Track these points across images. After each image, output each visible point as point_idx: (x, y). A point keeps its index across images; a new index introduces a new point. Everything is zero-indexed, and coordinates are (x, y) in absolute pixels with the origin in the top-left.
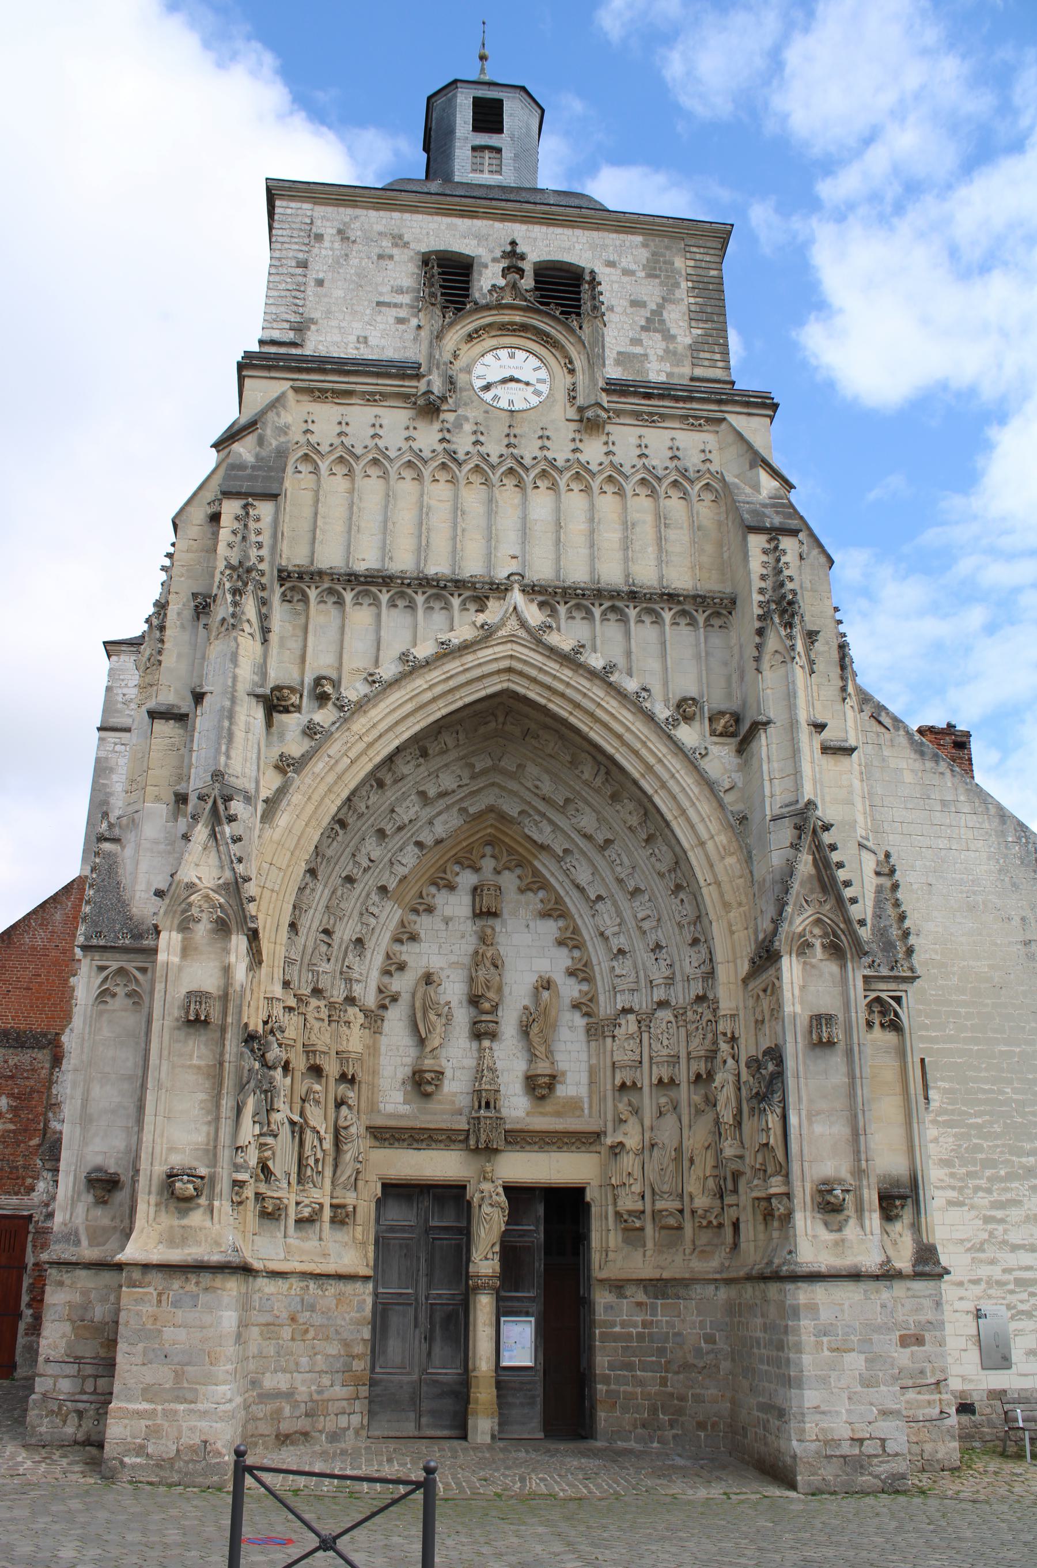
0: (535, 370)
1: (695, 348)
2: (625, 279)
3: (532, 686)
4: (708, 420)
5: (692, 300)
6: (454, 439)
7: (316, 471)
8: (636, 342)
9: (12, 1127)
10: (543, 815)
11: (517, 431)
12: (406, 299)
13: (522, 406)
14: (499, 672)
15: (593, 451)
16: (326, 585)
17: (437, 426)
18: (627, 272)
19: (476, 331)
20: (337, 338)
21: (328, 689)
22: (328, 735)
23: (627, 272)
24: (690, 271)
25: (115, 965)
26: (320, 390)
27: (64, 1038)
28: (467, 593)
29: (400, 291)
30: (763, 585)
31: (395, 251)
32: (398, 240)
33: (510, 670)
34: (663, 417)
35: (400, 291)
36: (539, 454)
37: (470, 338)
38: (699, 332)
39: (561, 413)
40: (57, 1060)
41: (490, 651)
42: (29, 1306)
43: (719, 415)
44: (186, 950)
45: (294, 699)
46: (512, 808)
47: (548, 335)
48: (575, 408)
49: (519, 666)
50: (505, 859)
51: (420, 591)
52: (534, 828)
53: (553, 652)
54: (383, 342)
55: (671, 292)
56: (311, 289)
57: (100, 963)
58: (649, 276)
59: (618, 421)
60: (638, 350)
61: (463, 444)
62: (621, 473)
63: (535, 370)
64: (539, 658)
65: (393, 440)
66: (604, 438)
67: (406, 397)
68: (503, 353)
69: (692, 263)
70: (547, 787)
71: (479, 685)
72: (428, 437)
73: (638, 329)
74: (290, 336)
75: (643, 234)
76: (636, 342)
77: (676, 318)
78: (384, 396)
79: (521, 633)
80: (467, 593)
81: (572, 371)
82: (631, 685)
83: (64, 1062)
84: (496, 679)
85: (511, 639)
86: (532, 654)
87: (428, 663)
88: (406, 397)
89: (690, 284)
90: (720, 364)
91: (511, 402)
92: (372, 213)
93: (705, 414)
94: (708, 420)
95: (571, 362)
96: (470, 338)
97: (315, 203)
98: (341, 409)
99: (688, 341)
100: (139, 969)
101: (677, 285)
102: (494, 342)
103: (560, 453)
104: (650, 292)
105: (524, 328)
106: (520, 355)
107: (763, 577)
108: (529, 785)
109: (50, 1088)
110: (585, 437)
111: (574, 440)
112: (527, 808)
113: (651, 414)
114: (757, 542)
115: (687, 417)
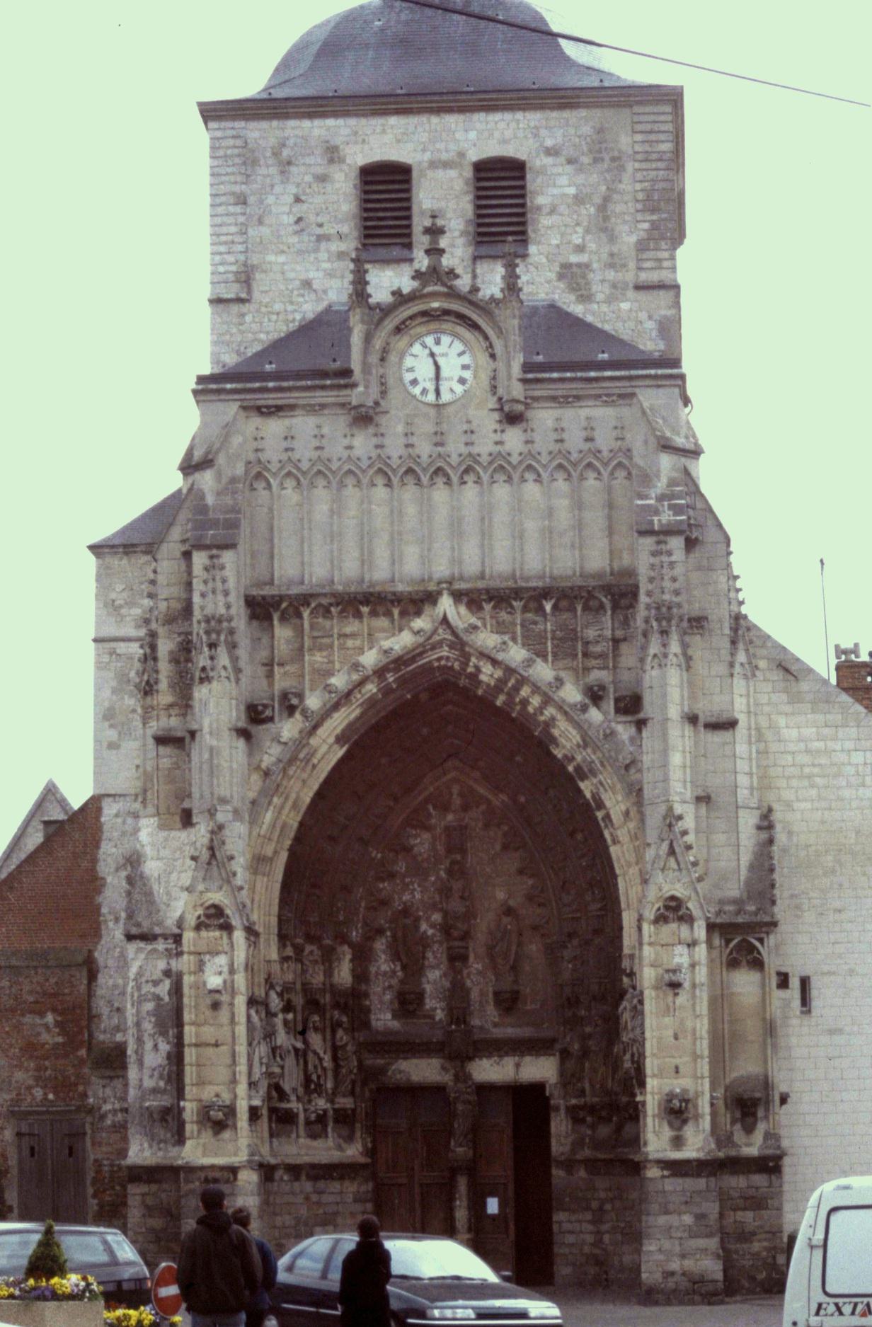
0: (460, 354)
1: (642, 247)
2: (569, 169)
4: (621, 396)
7: (269, 486)
8: (580, 249)
9: (60, 1039)
11: (445, 427)
15: (514, 439)
17: (371, 430)
21: (295, 701)
24: (638, 148)
27: (96, 954)
30: (650, 587)
34: (578, 398)
36: (464, 450)
37: (398, 330)
38: (646, 226)
40: (92, 976)
42: (95, 1196)
43: (629, 390)
45: (268, 713)
48: (495, 399)
58: (596, 161)
59: (535, 405)
60: (583, 258)
61: (395, 449)
63: (460, 354)
65: (336, 450)
72: (362, 443)
76: (580, 249)
77: (623, 207)
78: (323, 406)
81: (493, 356)
83: (100, 976)
88: (343, 405)
89: (637, 165)
92: (306, 123)
93: (617, 391)
94: (621, 396)
95: (491, 346)
96: (398, 330)
99: (633, 239)
103: (484, 447)
104: (594, 180)
107: (651, 580)
109: (89, 1002)
111: (495, 431)
113: (563, 397)
114: (649, 542)
115: (600, 396)
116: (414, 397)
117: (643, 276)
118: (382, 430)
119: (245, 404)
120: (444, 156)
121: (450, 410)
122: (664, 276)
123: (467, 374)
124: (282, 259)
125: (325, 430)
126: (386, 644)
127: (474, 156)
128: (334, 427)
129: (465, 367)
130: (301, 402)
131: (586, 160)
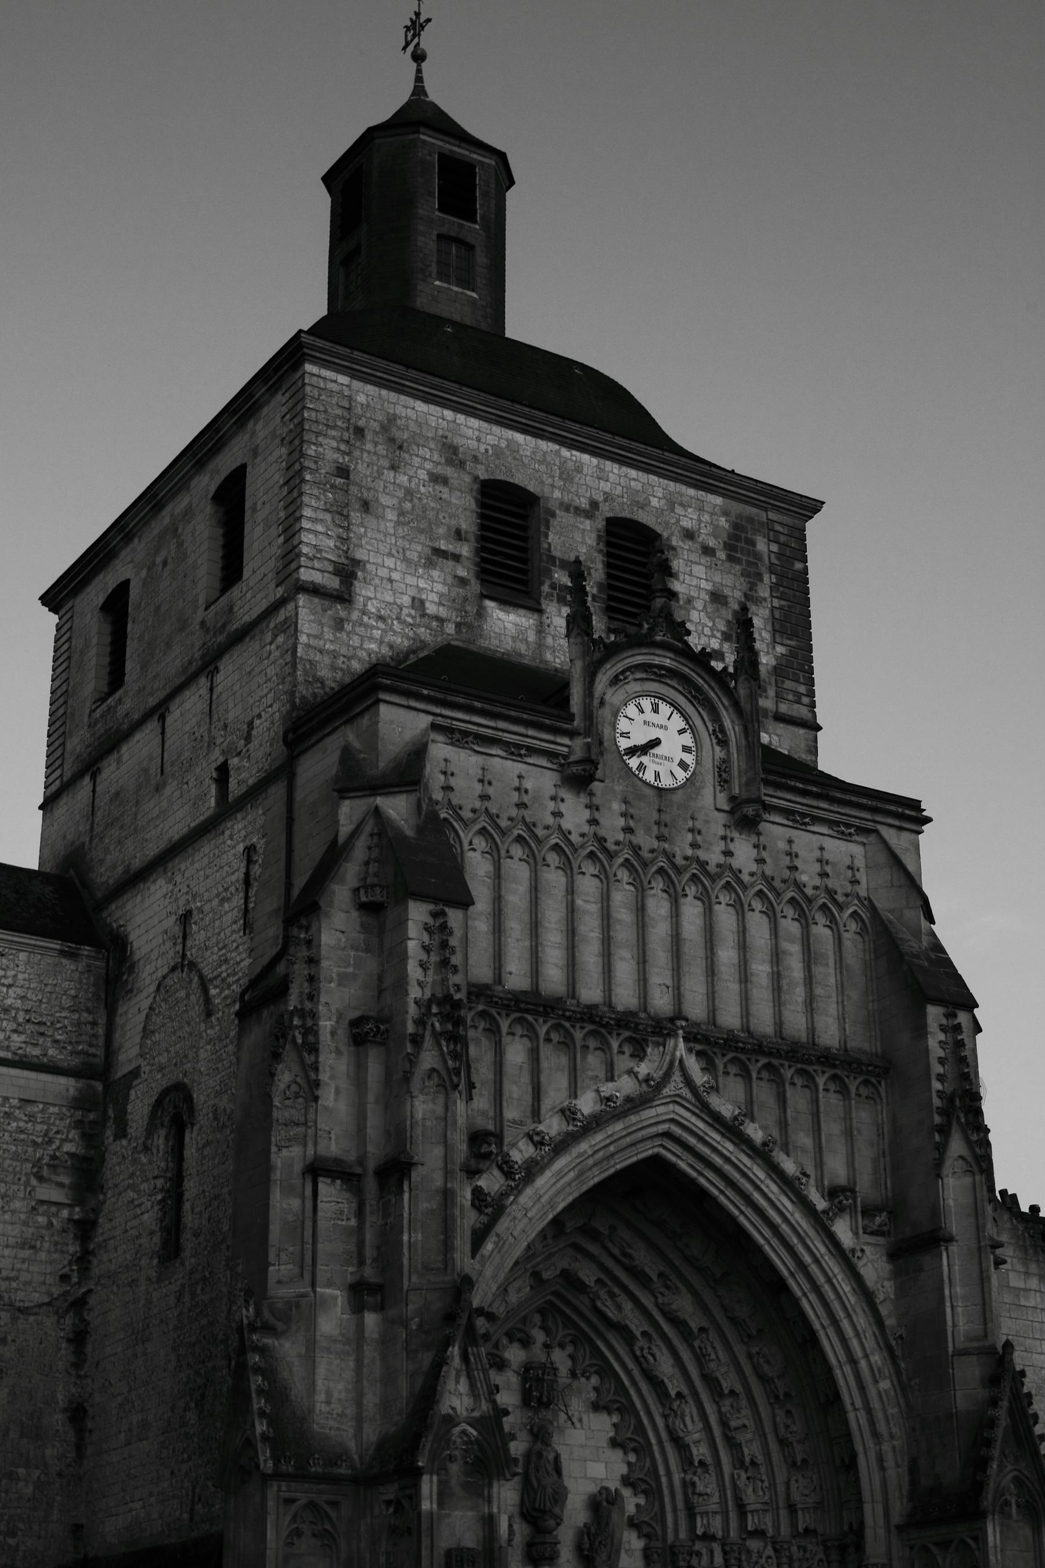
3: (686, 1155)
5: (776, 603)
6: (602, 821)
10: (624, 1288)
11: (666, 818)
12: (465, 550)
13: (666, 782)
14: (652, 1137)
16: (481, 1007)
18: (708, 551)
19: (623, 672)
20: (389, 598)
22: (499, 1210)
23: (708, 551)
25: (303, 1499)
26: (461, 731)
28: (627, 1034)
29: (459, 535)
30: (941, 1070)
31: (449, 471)
32: (452, 453)
33: (668, 1135)
34: (816, 820)
35: (459, 535)
39: (710, 800)
41: (652, 1112)
43: (870, 825)
44: (443, 1496)
46: (588, 1274)
47: (698, 689)
49: (677, 1131)
50: (561, 1334)
51: (578, 1025)
52: (609, 1303)
53: (716, 1119)
54: (443, 612)
55: (752, 587)
56: (356, 516)
57: (287, 1495)
58: (731, 559)
62: (773, 889)
64: (701, 1125)
66: (754, 839)
67: (551, 755)
68: (646, 703)
69: (774, 548)
70: (642, 1257)
71: (634, 1150)
72: (574, 815)
73: (719, 635)
74: (333, 583)
75: (723, 495)
78: (532, 751)
79: (686, 1092)
80: (627, 1034)
81: (723, 743)
82: (789, 1166)
84: (649, 1144)
85: (676, 1100)
86: (693, 1119)
87: (595, 1123)
88: (551, 755)
90: (805, 700)
91: (657, 775)
93: (857, 822)
97: (353, 377)
98: (480, 759)
100: (328, 1503)
101: (759, 577)
102: (635, 687)
103: (714, 857)
105: (672, 673)
106: (665, 709)
107: (941, 1061)
108: (616, 1251)
110: (736, 835)
112: (603, 1277)
113: (804, 815)
115: (837, 824)
116: (630, 769)
117: (783, 708)
118: (596, 801)
119: (440, 721)
120: (577, 502)
121: (678, 797)
122: (802, 712)
123: (689, 759)
124: (390, 562)
125: (528, 784)
126: (607, 1089)
127: (606, 511)
128: (542, 780)
129: (686, 749)
130: (507, 737)
131: (722, 555)
